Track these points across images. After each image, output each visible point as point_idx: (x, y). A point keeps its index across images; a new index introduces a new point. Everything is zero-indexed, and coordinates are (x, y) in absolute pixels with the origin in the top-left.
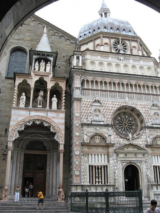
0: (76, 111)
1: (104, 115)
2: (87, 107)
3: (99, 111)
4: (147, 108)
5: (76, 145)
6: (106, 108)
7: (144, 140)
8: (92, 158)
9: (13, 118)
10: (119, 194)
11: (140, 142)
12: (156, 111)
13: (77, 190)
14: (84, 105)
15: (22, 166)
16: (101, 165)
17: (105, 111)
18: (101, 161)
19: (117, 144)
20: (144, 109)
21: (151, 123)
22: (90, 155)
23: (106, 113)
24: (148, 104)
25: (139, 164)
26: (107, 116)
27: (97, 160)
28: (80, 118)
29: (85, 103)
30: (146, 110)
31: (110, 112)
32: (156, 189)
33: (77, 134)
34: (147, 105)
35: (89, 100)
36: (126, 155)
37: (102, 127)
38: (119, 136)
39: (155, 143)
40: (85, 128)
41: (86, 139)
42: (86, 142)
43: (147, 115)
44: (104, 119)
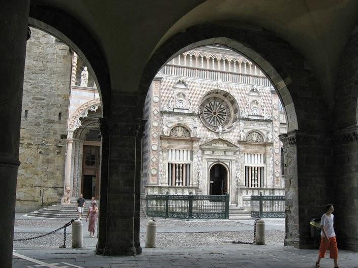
0: (154, 95)
1: (189, 100)
2: (168, 90)
3: (184, 95)
5: (154, 138)
6: (192, 92)
7: (237, 134)
8: (172, 154)
9: (73, 100)
10: (203, 198)
11: (232, 137)
12: (254, 98)
13: (153, 193)
14: (164, 87)
15: (81, 162)
16: (183, 163)
17: (191, 95)
18: (183, 158)
19: (204, 138)
20: (240, 95)
21: (247, 114)
22: (170, 151)
23: (192, 99)
25: (228, 164)
26: (193, 103)
27: (178, 157)
28: (159, 103)
29: (166, 84)
30: (242, 97)
31: (197, 98)
32: (246, 193)
33: (155, 124)
34: (245, 90)
35: (171, 81)
36: (213, 152)
37: (186, 116)
38: (206, 129)
39: (249, 139)
40: (165, 117)
41: (166, 131)
42: (166, 135)
43: (242, 102)
44: (189, 106)
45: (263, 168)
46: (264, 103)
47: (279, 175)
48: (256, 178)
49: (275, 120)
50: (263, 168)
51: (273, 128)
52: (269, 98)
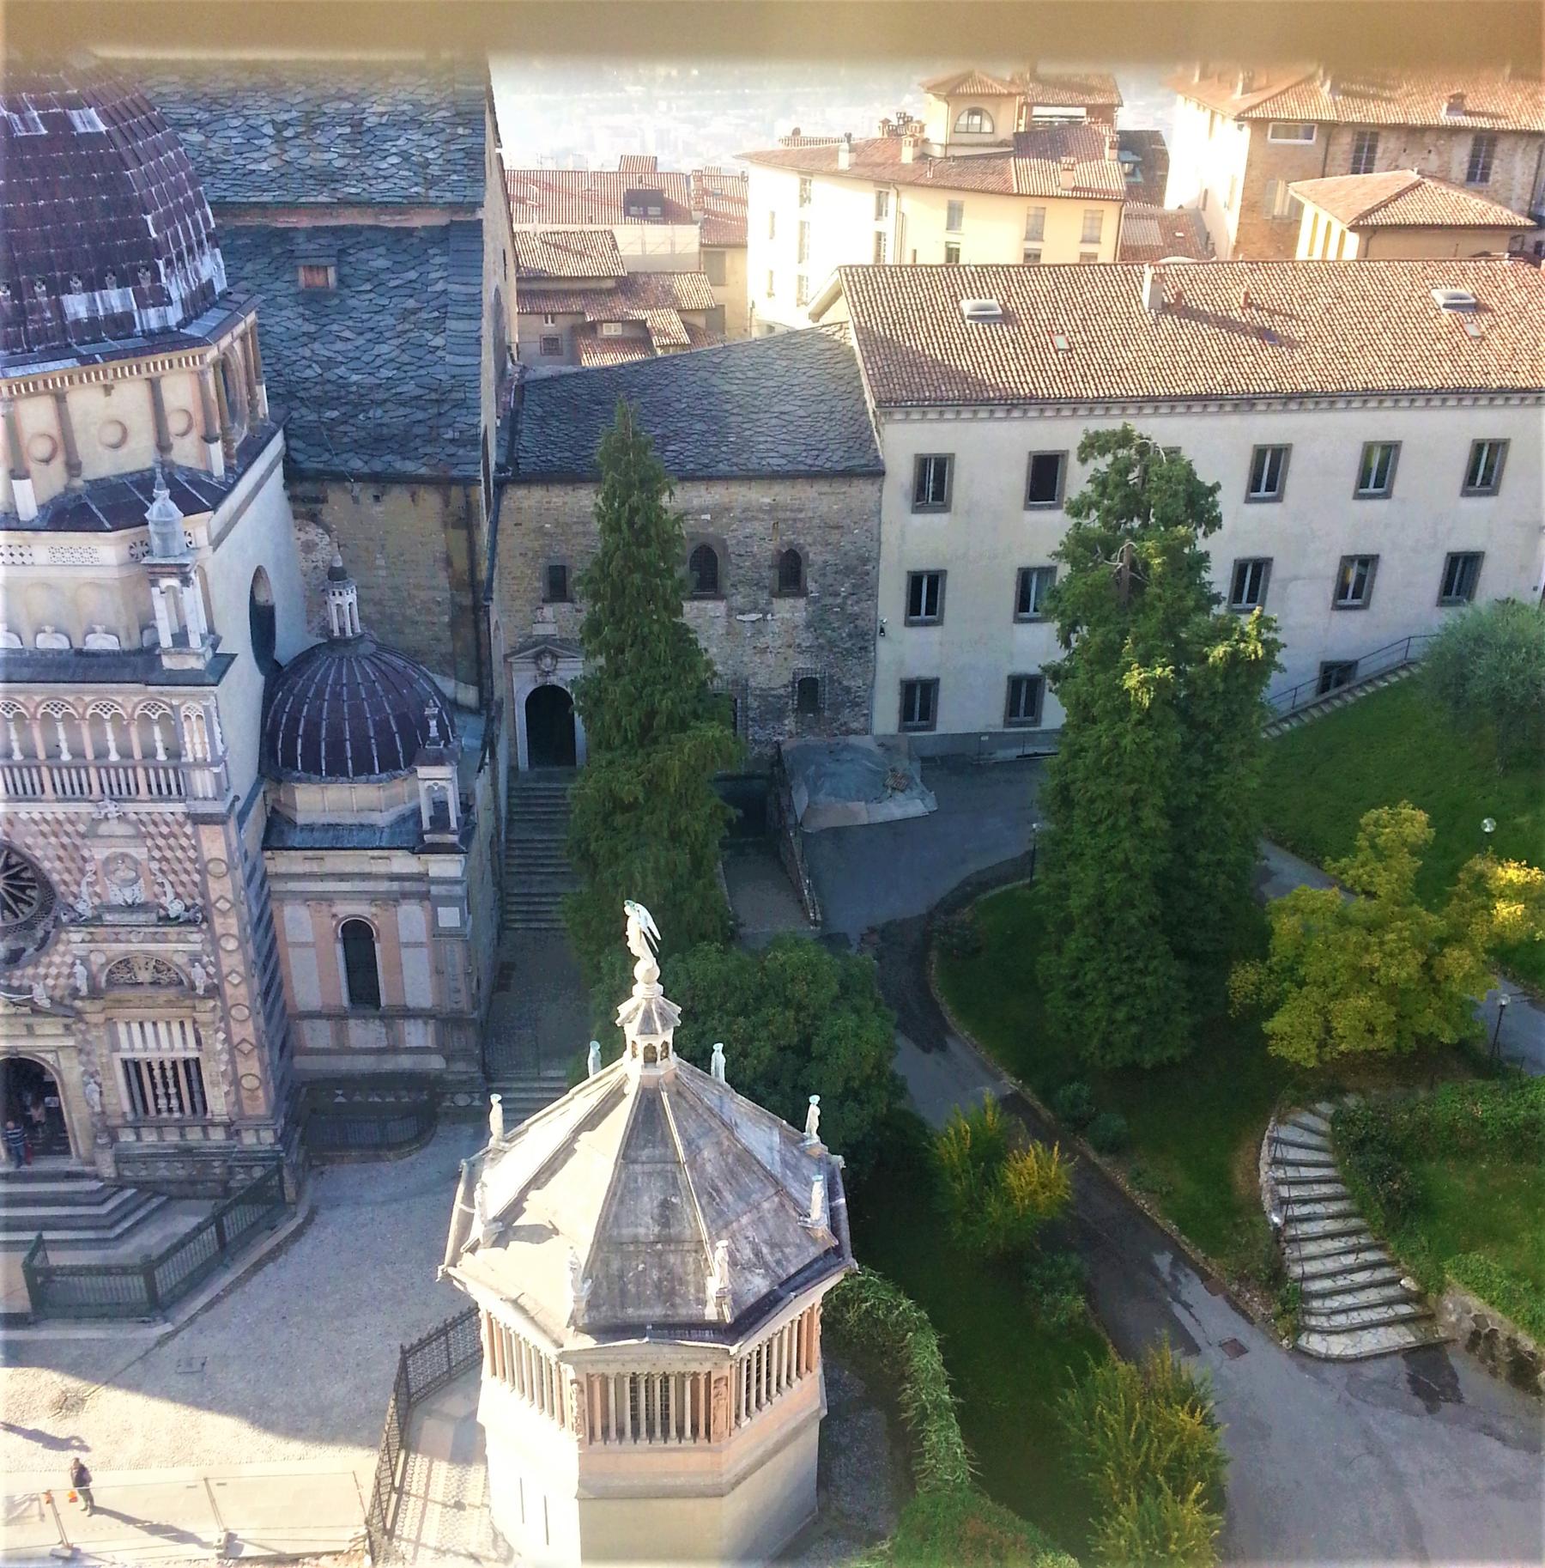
4: (67, 834)
7: (66, 971)
20: (53, 840)
21: (97, 901)
24: (73, 817)
25: (50, 1057)
30: (63, 846)
32: (132, 1138)
34: (72, 823)
45: (197, 1060)
46: (167, 860)
47: (256, 1083)
48: (172, 1090)
49: (223, 913)
50: (197, 1060)
51: (215, 941)
52: (184, 842)
